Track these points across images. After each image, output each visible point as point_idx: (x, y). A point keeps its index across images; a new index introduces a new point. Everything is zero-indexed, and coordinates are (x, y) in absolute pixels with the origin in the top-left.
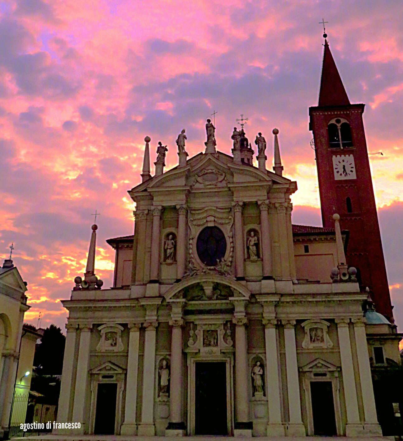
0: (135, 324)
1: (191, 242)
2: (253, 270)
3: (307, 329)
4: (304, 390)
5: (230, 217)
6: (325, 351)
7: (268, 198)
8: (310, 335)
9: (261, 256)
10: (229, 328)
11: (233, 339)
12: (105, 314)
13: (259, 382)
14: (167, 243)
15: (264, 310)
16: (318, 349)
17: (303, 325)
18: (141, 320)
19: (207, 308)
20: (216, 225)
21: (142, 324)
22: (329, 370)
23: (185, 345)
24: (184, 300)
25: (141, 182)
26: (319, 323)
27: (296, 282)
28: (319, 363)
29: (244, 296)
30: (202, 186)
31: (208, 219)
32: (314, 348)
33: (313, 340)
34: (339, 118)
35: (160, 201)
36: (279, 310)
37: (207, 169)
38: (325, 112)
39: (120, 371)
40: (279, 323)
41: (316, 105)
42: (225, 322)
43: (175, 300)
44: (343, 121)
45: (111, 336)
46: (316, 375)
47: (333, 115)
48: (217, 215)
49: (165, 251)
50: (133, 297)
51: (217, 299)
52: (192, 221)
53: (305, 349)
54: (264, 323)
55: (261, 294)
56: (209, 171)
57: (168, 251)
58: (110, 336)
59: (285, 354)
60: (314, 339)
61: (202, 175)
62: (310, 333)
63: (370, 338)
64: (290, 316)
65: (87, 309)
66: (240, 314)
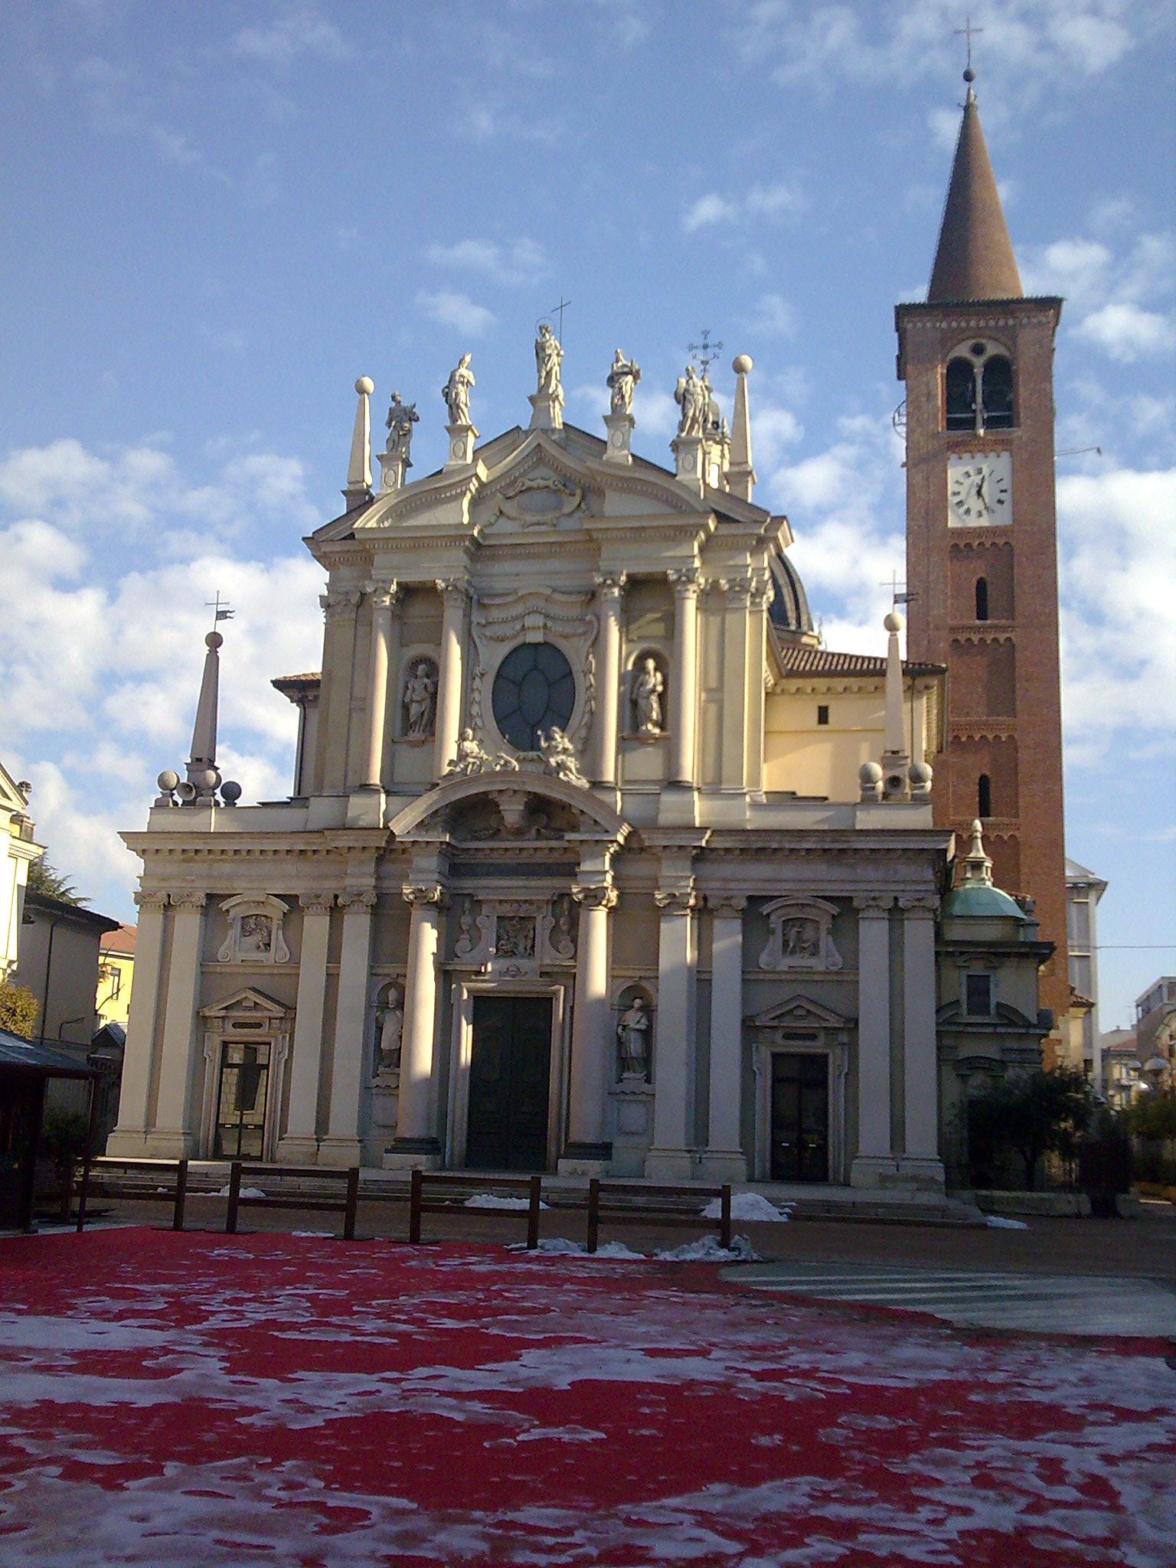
0: (318, 897)
1: (477, 682)
5: (588, 618)
6: (816, 977)
8: (784, 935)
11: (574, 941)
16: (802, 973)
17: (766, 910)
18: (330, 886)
19: (510, 859)
20: (551, 640)
21: (336, 897)
25: (345, 512)
26: (807, 905)
29: (607, 831)
31: (529, 621)
33: (789, 950)
36: (707, 869)
37: (530, 476)
38: (941, 322)
41: (919, 294)
42: (555, 898)
44: (992, 349)
45: (250, 925)
47: (963, 330)
48: (553, 610)
49: (406, 708)
50: (310, 827)
51: (539, 836)
52: (484, 626)
53: (765, 972)
56: (534, 484)
57: (414, 709)
58: (253, 926)
60: (794, 947)
61: (515, 496)
62: (784, 930)
63: (946, 952)
64: (732, 885)
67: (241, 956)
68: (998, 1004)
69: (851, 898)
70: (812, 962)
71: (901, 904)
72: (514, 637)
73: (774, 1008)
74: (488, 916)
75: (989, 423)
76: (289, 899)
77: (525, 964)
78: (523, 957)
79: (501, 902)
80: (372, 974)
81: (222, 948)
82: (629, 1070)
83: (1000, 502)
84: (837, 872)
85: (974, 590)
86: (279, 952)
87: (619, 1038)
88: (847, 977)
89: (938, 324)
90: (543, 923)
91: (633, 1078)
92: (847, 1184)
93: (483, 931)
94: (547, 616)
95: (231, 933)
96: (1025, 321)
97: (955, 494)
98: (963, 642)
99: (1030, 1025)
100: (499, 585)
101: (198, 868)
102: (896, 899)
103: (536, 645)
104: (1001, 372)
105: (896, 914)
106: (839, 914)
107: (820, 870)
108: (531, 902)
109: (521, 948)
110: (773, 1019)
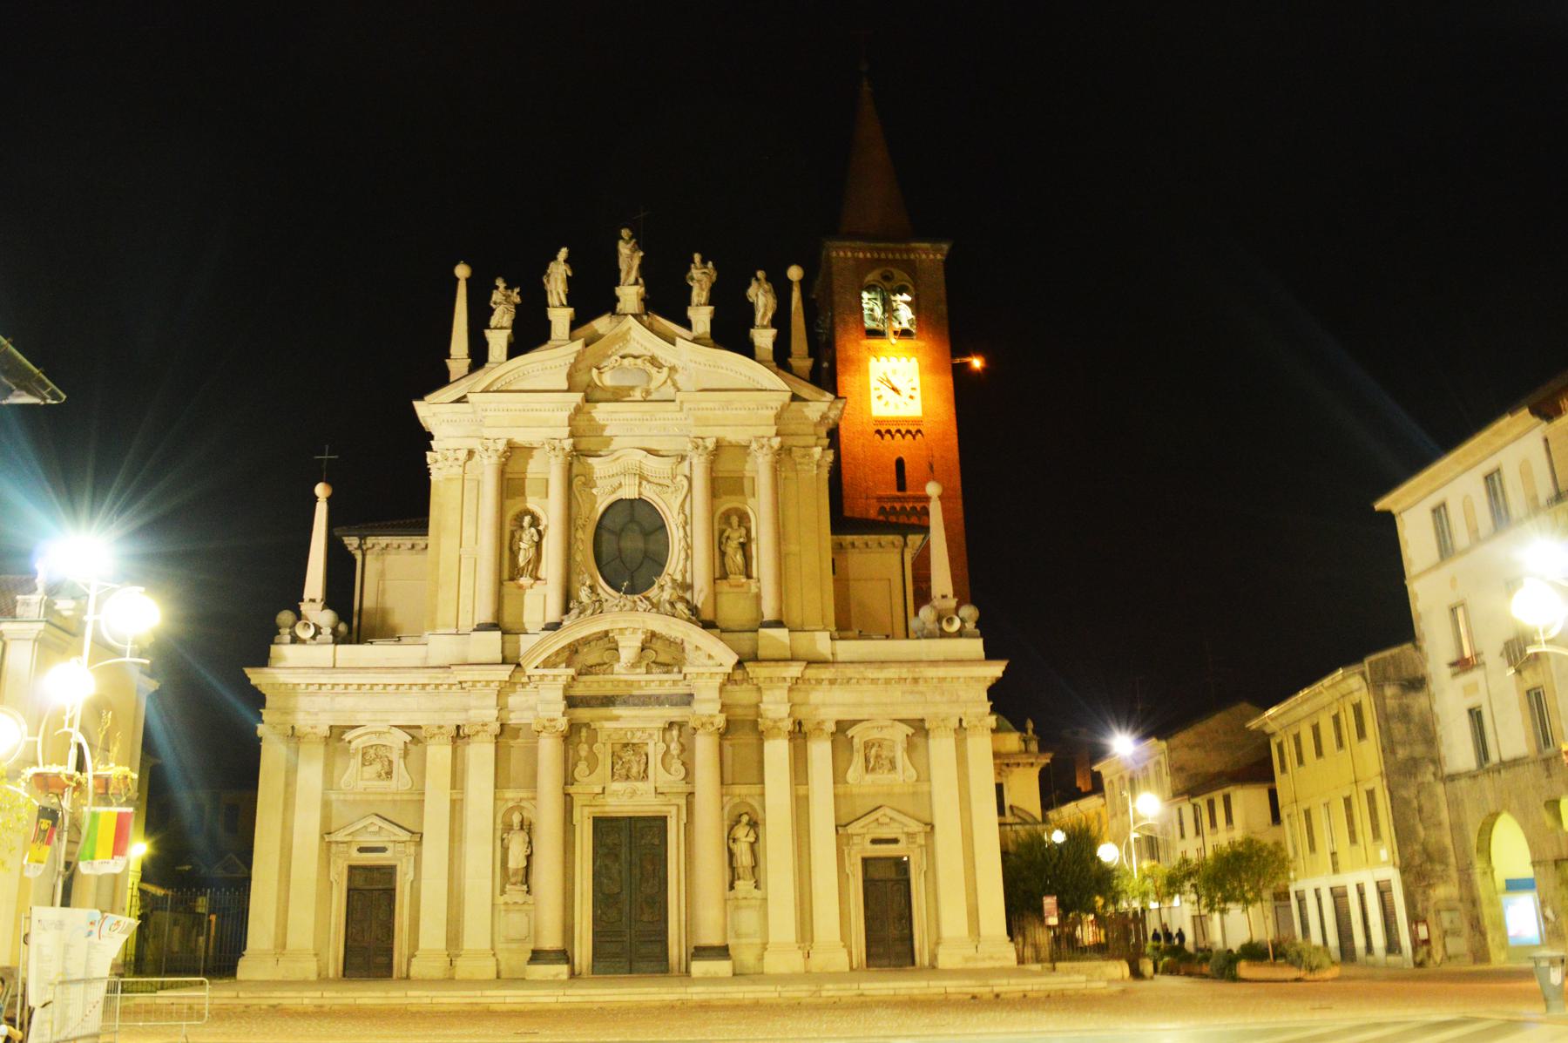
0: (440, 727)
3: (858, 743)
4: (848, 875)
7: (777, 435)
9: (755, 574)
10: (676, 739)
13: (744, 859)
14: (517, 536)
15: (765, 698)
22: (906, 830)
23: (569, 779)
28: (885, 815)
33: (871, 766)
34: (892, 270)
36: (798, 697)
38: (858, 252)
39: (405, 836)
40: (797, 728)
43: (546, 671)
54: (761, 728)
59: (807, 797)
67: (362, 784)
70: (892, 776)
71: (964, 724)
74: (604, 744)
77: (640, 785)
78: (636, 779)
80: (495, 799)
81: (345, 777)
82: (739, 879)
83: (911, 397)
85: (894, 467)
86: (402, 780)
87: (730, 850)
89: (856, 254)
90: (655, 750)
91: (744, 886)
93: (600, 757)
94: (642, 477)
95: (352, 761)
96: (924, 256)
97: (876, 389)
98: (888, 510)
102: (961, 720)
103: (632, 501)
106: (913, 734)
108: (643, 730)
110: (863, 827)
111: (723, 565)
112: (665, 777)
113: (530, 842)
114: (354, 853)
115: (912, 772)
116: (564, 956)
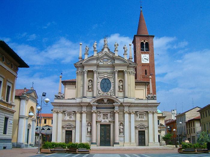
2: (121, 94)
3: (138, 115)
12: (67, 108)
24: (97, 104)
27: (135, 99)
30: (102, 63)
31: (105, 75)
32: (141, 120)
35: (87, 69)
36: (130, 108)
46: (140, 128)
49: (88, 86)
51: (108, 104)
54: (124, 112)
55: (124, 103)
57: (90, 87)
65: (60, 106)
66: (117, 109)
68: (160, 124)
69: (148, 112)
72: (103, 78)
73: (138, 125)
75: (146, 50)
76: (75, 112)
77: (106, 120)
79: (103, 112)
84: (146, 108)
87: (119, 129)
88: (148, 121)
90: (109, 115)
92: (148, 146)
99: (164, 126)
100: (100, 71)
101: (61, 108)
104: (147, 44)
105: (153, 113)
107: (144, 108)
108: (107, 112)
109: (106, 118)
111: (119, 88)
112: (110, 119)
113: (91, 128)
114: (66, 129)
115: (146, 119)
116: (95, 144)
